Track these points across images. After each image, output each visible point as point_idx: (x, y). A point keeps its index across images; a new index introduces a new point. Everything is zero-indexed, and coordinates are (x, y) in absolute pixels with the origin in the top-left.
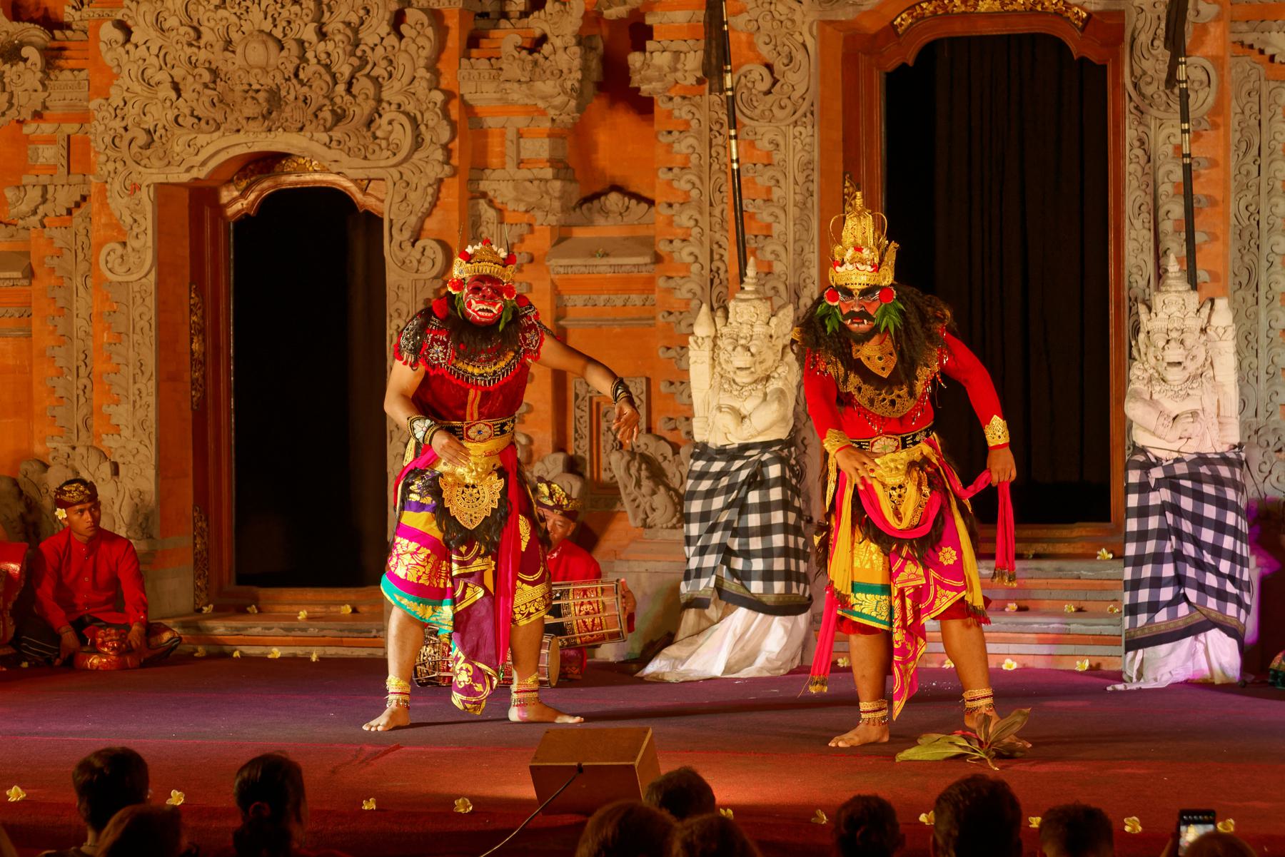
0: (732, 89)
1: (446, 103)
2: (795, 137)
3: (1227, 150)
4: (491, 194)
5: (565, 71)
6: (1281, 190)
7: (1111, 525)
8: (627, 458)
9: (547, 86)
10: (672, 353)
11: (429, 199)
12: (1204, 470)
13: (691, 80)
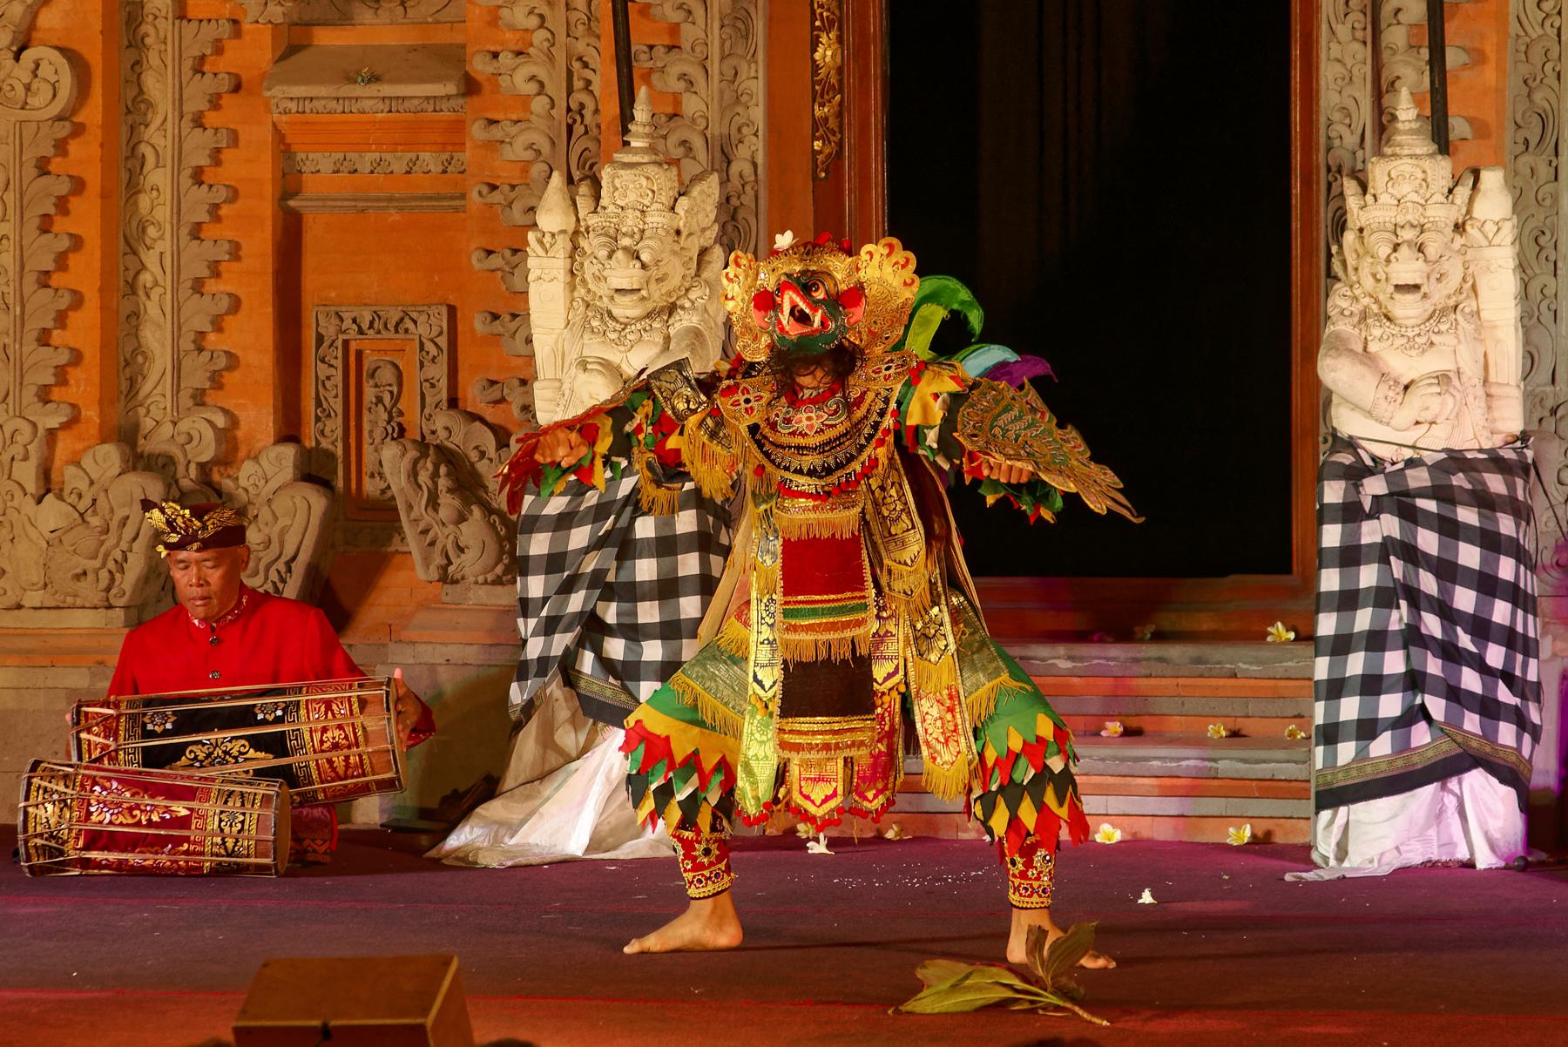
7: (1292, 580)
8: (412, 454)
10: (496, 261)
12: (1459, 480)
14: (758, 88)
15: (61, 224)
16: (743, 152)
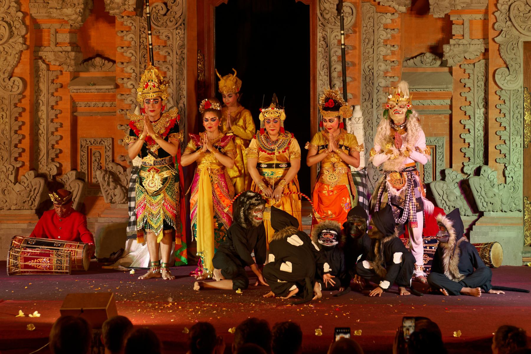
0: (149, 13)
1: (24, 17)
2: (177, 34)
3: (360, 42)
4: (44, 57)
5: (77, 4)
6: (382, 59)
8: (104, 173)
9: (69, 11)
10: (123, 127)
11: (16, 59)
13: (131, 9)
14: (184, 86)
15: (20, 119)
16: (181, 102)
